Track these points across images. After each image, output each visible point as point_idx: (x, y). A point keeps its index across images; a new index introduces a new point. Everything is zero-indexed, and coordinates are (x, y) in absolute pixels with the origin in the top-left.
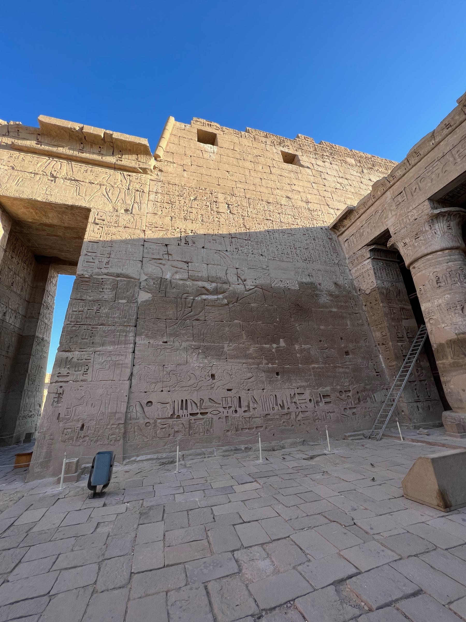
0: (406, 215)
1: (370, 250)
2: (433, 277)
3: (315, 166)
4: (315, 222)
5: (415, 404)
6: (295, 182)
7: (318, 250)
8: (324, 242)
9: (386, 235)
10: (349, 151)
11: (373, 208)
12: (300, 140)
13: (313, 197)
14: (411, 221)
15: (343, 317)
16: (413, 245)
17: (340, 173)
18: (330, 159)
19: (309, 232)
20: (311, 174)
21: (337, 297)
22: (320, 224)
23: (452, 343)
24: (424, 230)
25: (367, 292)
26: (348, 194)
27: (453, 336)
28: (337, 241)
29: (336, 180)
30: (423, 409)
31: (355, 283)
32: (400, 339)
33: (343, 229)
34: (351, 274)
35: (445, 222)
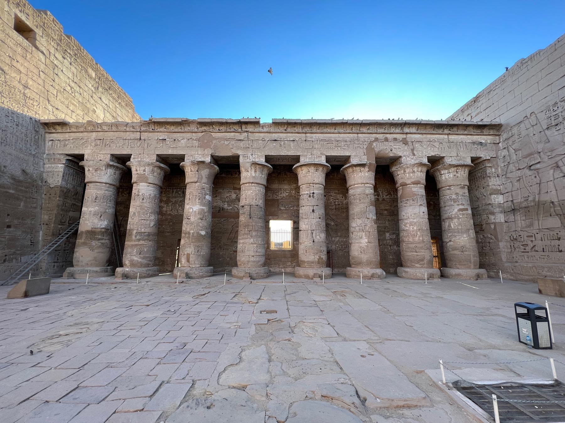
1: (67, 160)
2: (94, 196)
3: (52, 58)
4: (26, 109)
5: (53, 264)
6: (19, 58)
7: (17, 136)
8: (28, 132)
9: (81, 157)
10: (94, 63)
12: (47, 19)
13: (35, 85)
15: (18, 199)
17: (75, 78)
19: (15, 116)
20: (43, 60)
21: (20, 181)
22: (31, 114)
23: (88, 232)
25: (52, 186)
27: (89, 229)
28: (43, 136)
30: (57, 267)
31: (45, 175)
32: (62, 223)
33: (53, 131)
34: (44, 168)
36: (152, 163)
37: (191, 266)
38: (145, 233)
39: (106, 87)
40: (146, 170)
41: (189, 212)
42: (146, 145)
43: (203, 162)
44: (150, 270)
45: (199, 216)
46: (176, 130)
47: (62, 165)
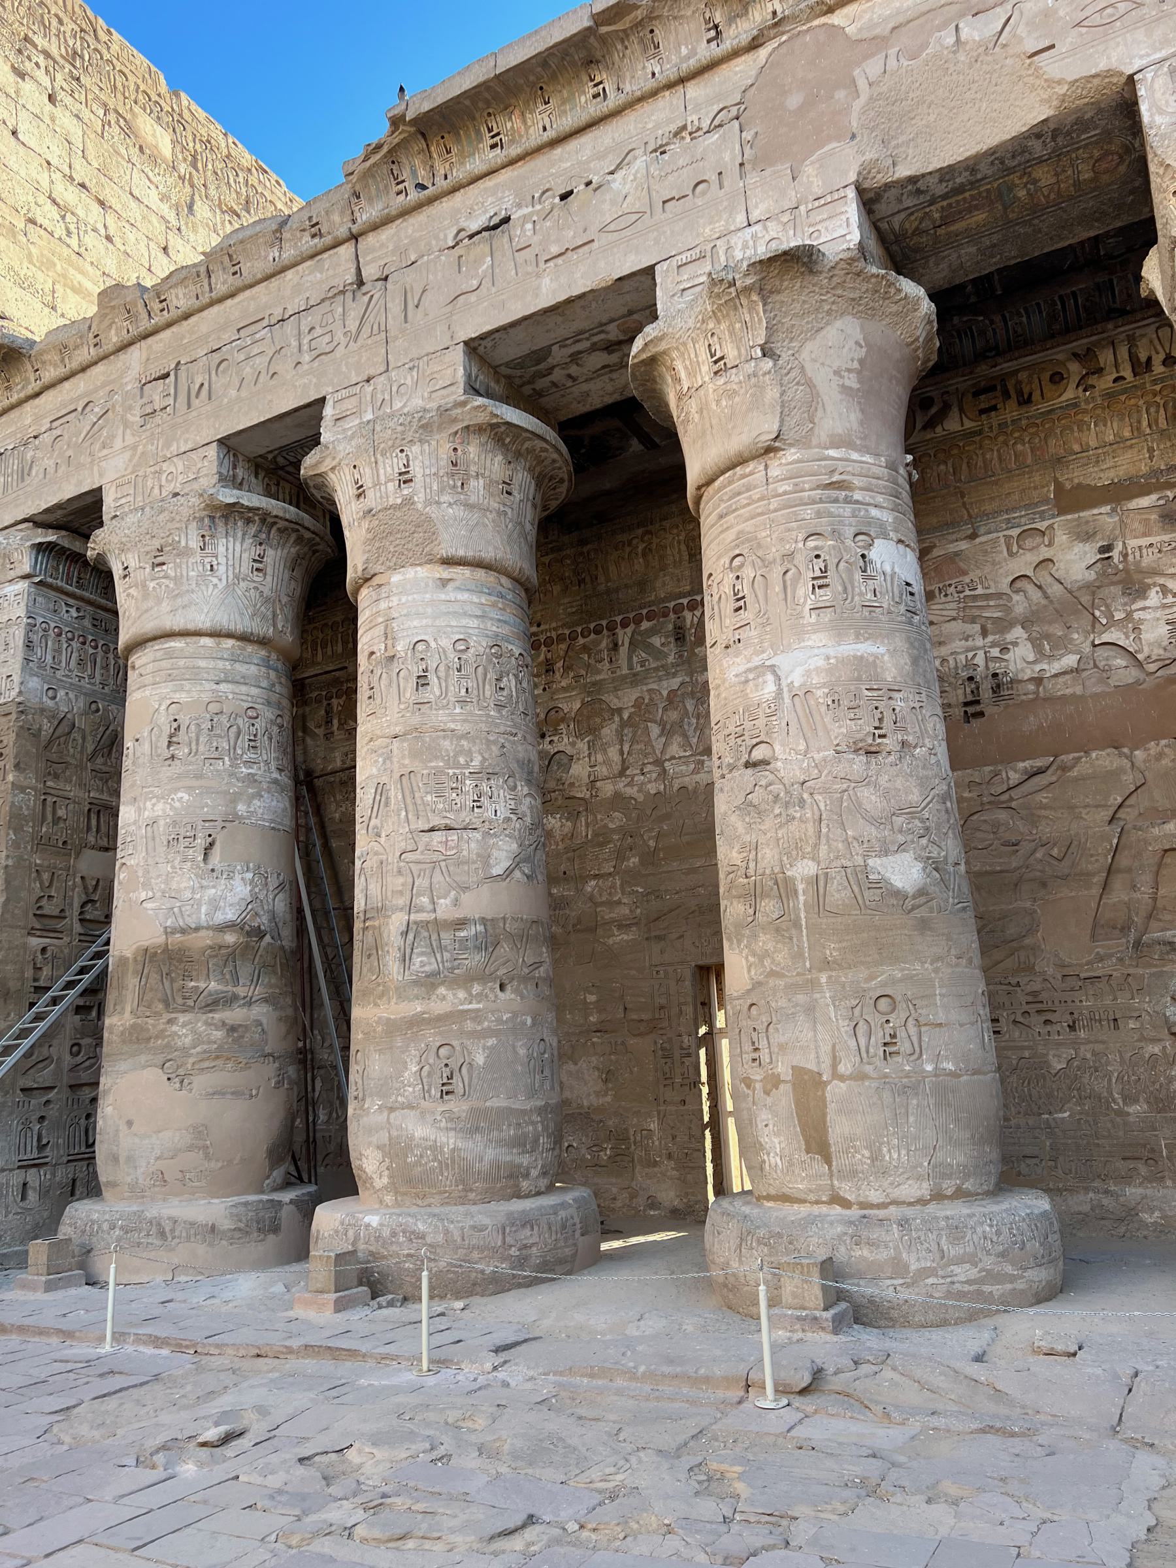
0: (157, 468)
1: (40, 548)
2: (163, 720)
5: (17, 1178)
11: (79, 386)
14: (164, 494)
16: (144, 586)
17: (78, 163)
18: (59, 77)
23: (149, 957)
24: (183, 543)
26: (82, 272)
29: (45, 184)
30: (44, 1193)
35: (249, 541)
36: (443, 411)
37: (846, 1190)
38: (461, 923)
39: (231, 200)
40: (416, 469)
41: (750, 712)
42: (395, 307)
43: (798, 262)
44: (527, 1222)
45: (841, 729)
46: (568, 122)
47: (23, 585)
